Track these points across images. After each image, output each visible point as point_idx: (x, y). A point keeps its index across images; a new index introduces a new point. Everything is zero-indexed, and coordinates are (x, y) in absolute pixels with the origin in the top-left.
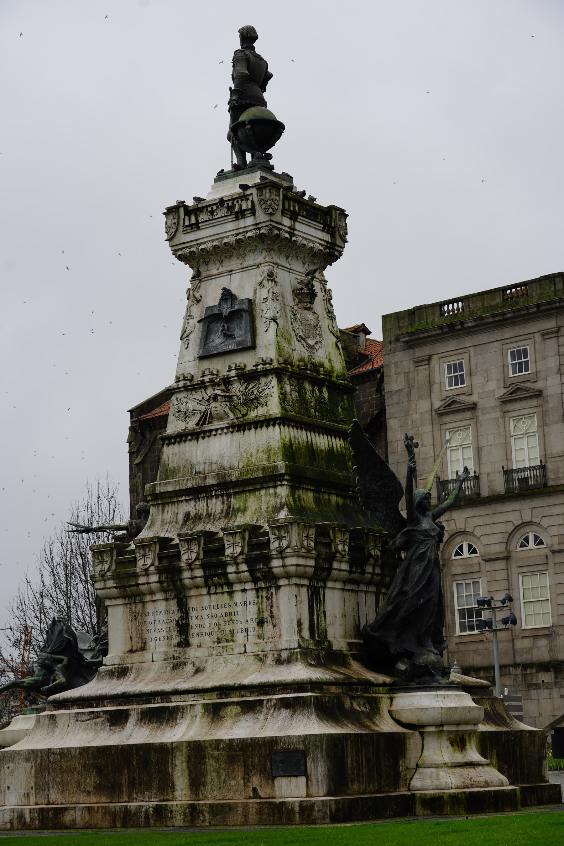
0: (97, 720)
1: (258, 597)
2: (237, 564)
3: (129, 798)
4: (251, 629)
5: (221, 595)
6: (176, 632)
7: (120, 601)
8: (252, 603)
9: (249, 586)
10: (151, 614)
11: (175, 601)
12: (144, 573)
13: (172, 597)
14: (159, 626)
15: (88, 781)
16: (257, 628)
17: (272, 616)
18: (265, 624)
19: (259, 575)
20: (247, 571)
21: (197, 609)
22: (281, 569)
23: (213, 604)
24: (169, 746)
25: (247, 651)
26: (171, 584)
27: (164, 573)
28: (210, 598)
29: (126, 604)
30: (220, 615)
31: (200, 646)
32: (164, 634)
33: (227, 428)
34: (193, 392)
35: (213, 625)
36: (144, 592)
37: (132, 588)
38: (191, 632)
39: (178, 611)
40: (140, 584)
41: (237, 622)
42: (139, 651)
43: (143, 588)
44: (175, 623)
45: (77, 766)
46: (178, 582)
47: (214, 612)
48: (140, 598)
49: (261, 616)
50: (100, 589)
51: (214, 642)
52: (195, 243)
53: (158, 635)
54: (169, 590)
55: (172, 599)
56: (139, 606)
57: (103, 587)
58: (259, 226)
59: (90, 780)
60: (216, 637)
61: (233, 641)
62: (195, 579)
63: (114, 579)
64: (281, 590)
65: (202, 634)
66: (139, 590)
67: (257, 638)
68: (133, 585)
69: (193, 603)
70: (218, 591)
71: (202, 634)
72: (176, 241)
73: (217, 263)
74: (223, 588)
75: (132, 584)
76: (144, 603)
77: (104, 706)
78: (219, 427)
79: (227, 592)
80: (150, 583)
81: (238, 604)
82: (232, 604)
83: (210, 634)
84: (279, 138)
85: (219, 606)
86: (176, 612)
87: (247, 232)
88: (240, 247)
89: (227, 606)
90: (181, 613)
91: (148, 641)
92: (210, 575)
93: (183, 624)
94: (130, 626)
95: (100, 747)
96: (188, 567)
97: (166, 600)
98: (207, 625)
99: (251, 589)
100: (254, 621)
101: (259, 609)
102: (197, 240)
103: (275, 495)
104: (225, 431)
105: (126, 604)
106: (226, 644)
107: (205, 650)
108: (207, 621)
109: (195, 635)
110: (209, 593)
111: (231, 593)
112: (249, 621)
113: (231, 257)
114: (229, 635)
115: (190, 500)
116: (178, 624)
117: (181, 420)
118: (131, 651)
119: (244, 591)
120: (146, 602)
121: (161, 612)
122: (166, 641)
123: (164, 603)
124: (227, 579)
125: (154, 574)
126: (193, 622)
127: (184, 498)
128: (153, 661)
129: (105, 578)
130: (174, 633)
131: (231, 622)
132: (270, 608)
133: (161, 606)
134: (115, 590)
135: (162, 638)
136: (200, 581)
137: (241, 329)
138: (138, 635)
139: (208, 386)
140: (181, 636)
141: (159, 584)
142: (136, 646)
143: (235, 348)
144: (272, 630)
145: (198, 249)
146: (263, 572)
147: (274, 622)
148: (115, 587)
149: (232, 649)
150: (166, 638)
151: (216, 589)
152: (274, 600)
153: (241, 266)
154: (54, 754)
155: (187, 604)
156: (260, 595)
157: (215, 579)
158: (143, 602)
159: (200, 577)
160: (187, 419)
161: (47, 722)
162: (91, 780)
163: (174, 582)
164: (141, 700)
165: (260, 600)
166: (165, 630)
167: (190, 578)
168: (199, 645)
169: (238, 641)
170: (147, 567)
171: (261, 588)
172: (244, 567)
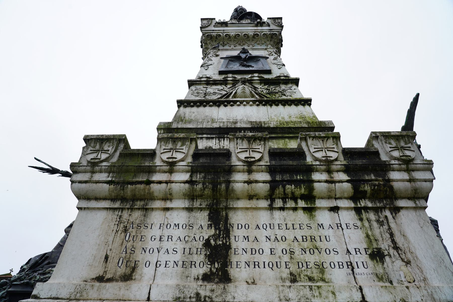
1: (361, 220)
2: (329, 172)
4: (360, 264)
5: (291, 212)
6: (202, 256)
8: (351, 226)
11: (205, 214)
12: (167, 168)
13: (204, 206)
14: (168, 245)
16: (370, 263)
17: (396, 248)
18: (387, 258)
19: (367, 188)
20: (348, 181)
21: (247, 227)
22: (407, 184)
23: (276, 223)
26: (210, 186)
27: (200, 172)
28: (272, 214)
29: (114, 209)
30: (292, 238)
31: (253, 283)
32: (178, 257)
33: (254, 102)
36: (156, 194)
37: (138, 186)
38: (234, 259)
39: (210, 226)
40: (153, 182)
41: (328, 251)
42: (117, 281)
44: (201, 243)
46: (223, 186)
47: (280, 233)
48: (142, 203)
49: (375, 246)
51: (283, 280)
53: (163, 258)
54: (201, 196)
56: (137, 215)
60: (287, 271)
61: (323, 280)
62: (254, 185)
63: (109, 173)
65: (256, 265)
66: (149, 190)
67: (376, 279)
68: (141, 183)
70: (288, 205)
71: (256, 265)
74: (296, 203)
75: (140, 179)
76: (146, 210)
79: (304, 209)
82: (314, 226)
83: (276, 265)
85: (290, 225)
86: (205, 228)
89: (305, 226)
90: (216, 229)
91: (141, 265)
92: (283, 181)
93: (216, 246)
94: (111, 239)
96: (246, 168)
97: (190, 210)
99: (348, 209)
100: (363, 252)
101: (368, 236)
104: (251, 103)
105: (114, 209)
106: (310, 284)
107: (270, 289)
108: (266, 246)
109: (243, 264)
110: (271, 208)
111: (310, 211)
112: (353, 252)
114: (315, 271)
115: (212, 138)
116: (207, 244)
118: (100, 279)
119: (335, 209)
120: (153, 209)
121: (177, 226)
122: (179, 269)
124: (311, 189)
125: (183, 171)
127: (205, 136)
129: (97, 168)
130: (199, 258)
131: (316, 251)
132: (388, 236)
134: (106, 186)
135: (171, 264)
136: (263, 188)
138: (124, 255)
140: (212, 263)
141: (187, 185)
142: (113, 271)
144: (404, 268)
146: (375, 185)
147: (403, 257)
148: (109, 182)
149: (333, 293)
150: (180, 263)
151: (285, 202)
152: (393, 225)
155: (227, 218)
157: (290, 188)
158: (147, 209)
159: (264, 182)
163: (215, 185)
165: (366, 224)
166: (180, 251)
167: (245, 182)
168: (250, 281)
169: (334, 280)
171: (366, 209)
172: (343, 176)
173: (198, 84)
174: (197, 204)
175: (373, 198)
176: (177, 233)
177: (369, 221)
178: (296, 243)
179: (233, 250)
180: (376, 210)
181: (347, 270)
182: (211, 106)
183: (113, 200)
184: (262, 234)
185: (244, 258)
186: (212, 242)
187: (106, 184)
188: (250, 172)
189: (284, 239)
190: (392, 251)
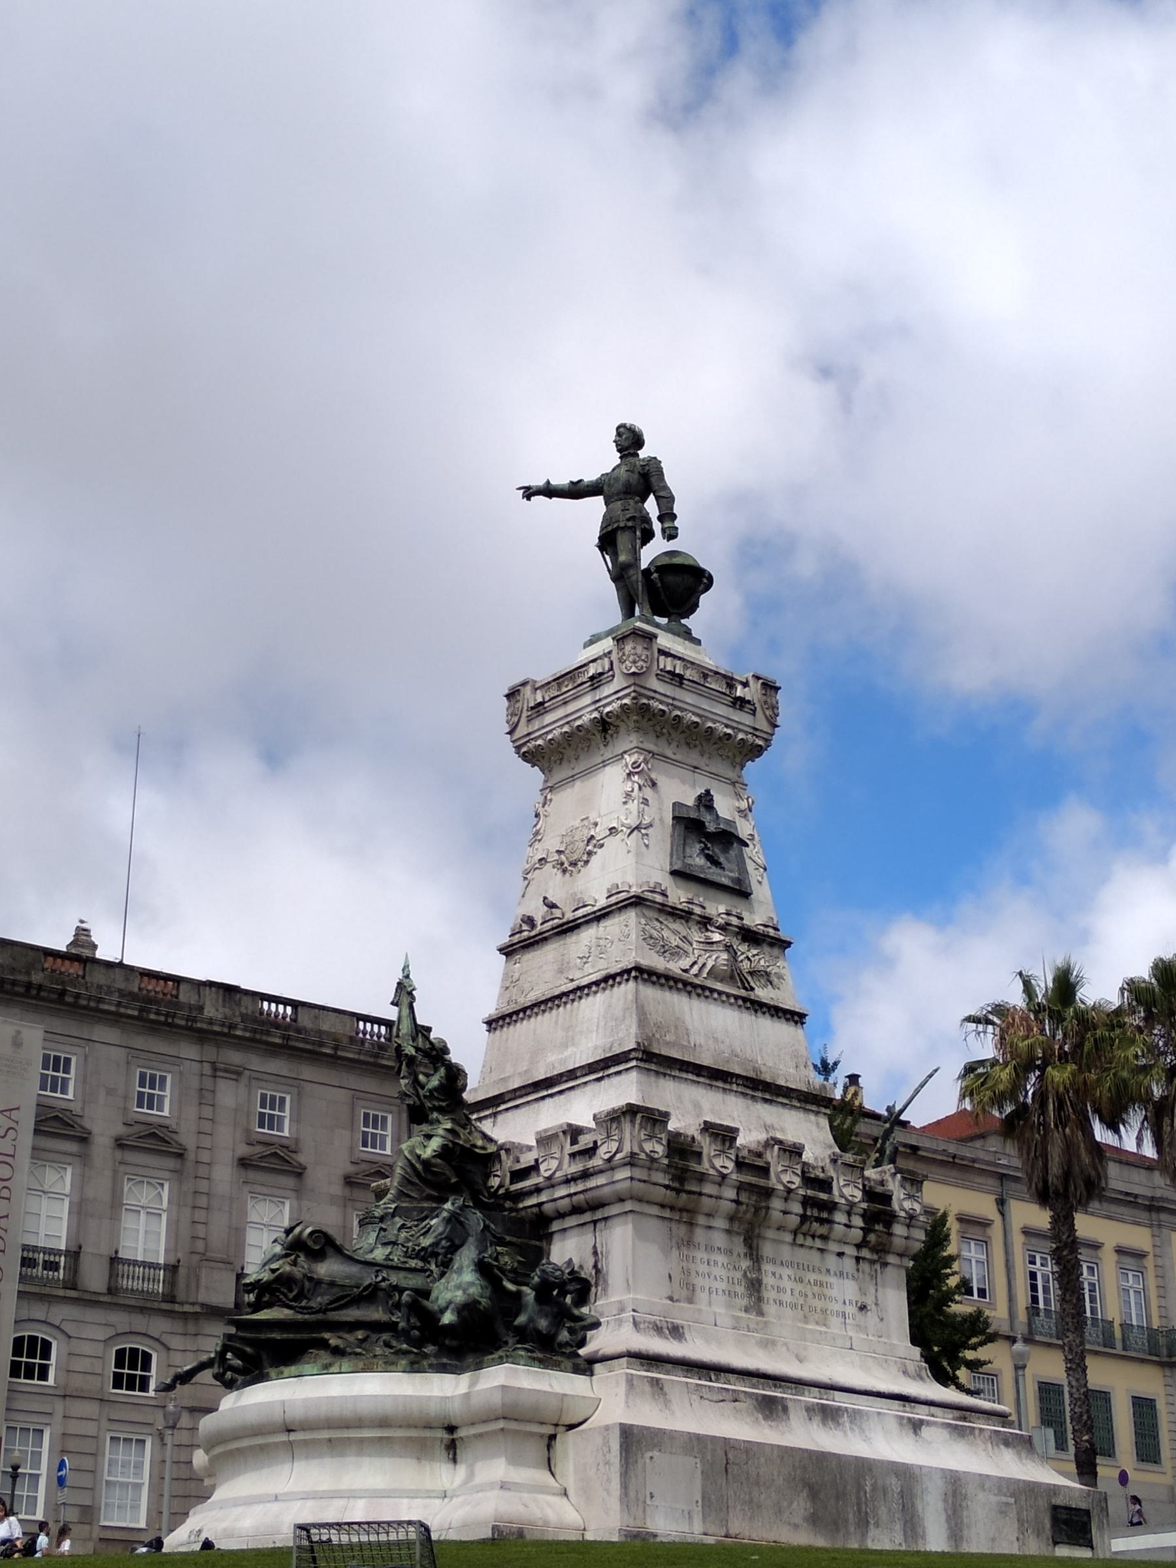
6: (743, 1288)
9: (851, 1251)
35: (796, 1293)
38: (765, 1294)
41: (831, 1299)
50: (640, 1180)
55: (738, 1233)
85: (806, 1266)
86: (742, 1256)
99: (851, 1256)
119: (840, 1254)
121: (719, 1249)
126: (768, 1280)
130: (740, 1289)
133: (719, 1239)
135: (720, 1292)
166: (726, 1280)
171: (864, 1259)
175: (873, 1250)
178: (809, 1286)
179: (763, 1286)
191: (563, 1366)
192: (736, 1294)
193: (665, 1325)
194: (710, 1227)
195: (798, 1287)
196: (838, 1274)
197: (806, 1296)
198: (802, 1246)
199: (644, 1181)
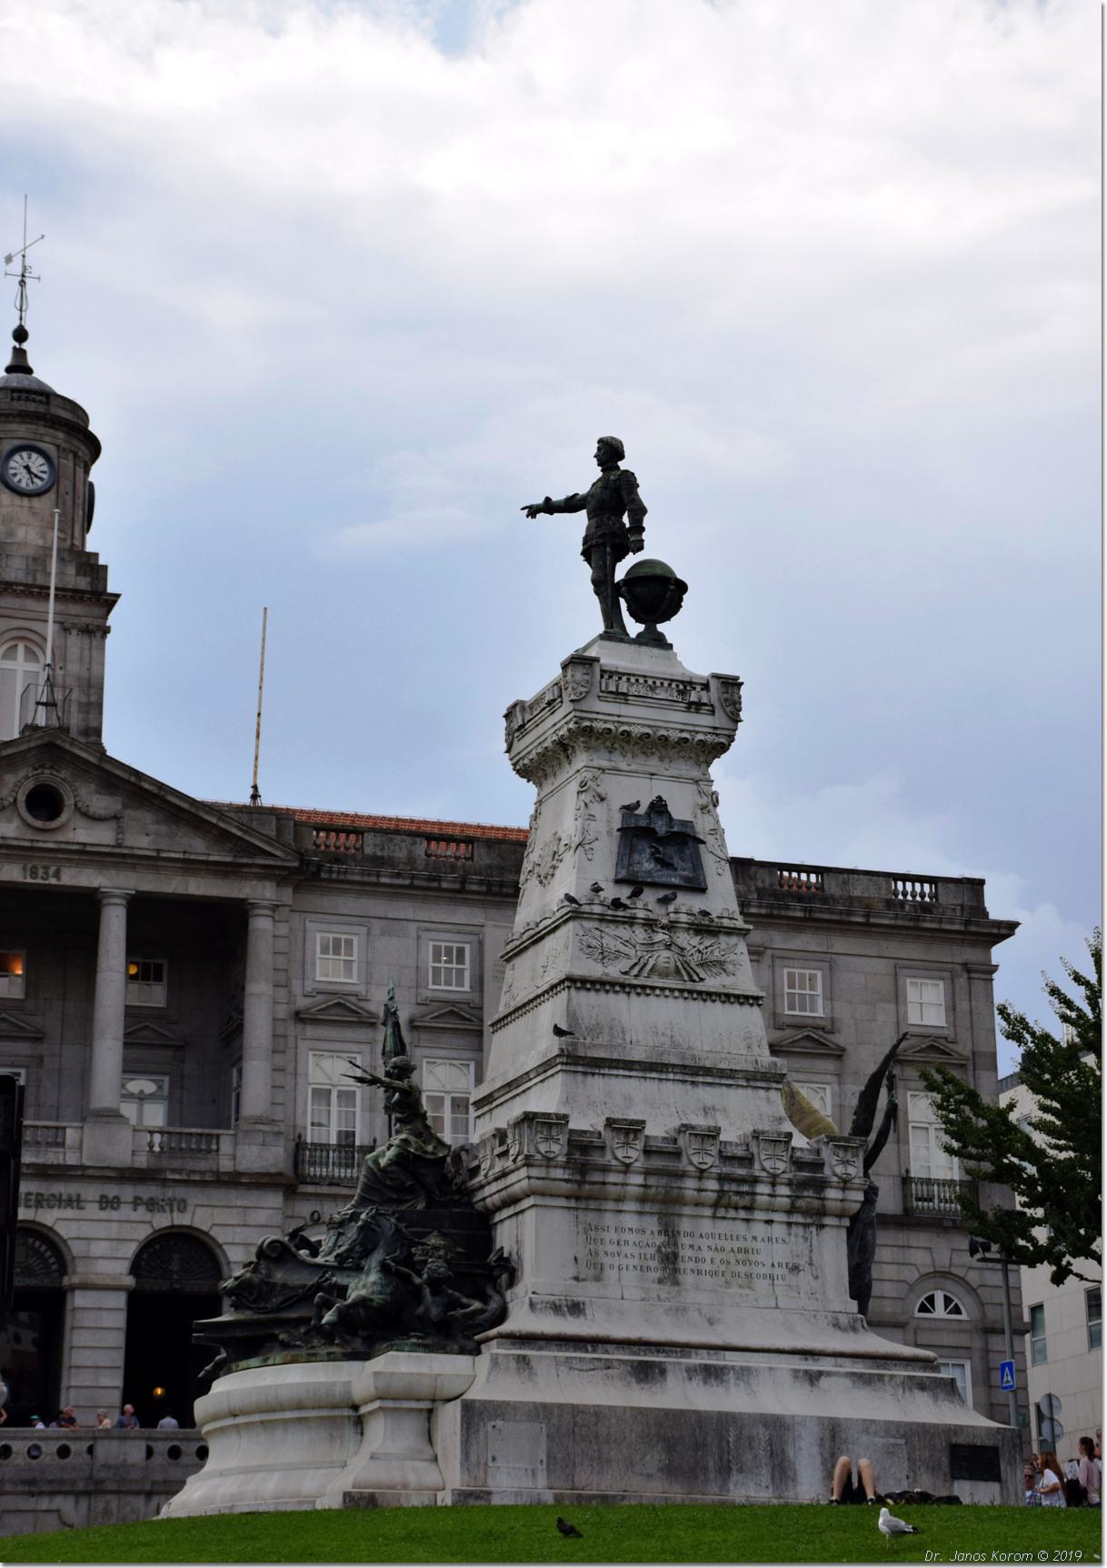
0: (609, 1371)
1: (790, 1234)
2: (773, 1185)
3: (721, 1490)
7: (562, 1202)
10: (612, 1230)
14: (627, 1250)
15: (648, 1458)
17: (811, 1264)
20: (788, 1196)
21: (692, 1235)
22: (839, 1203)
24: (788, 1422)
25: (780, 1306)
29: (569, 1208)
33: (681, 991)
34: (612, 926)
38: (681, 1266)
41: (757, 1263)
43: (611, 1188)
45: (627, 1434)
47: (720, 1243)
52: (616, 719)
53: (624, 1262)
57: (543, 1176)
58: (718, 732)
59: (652, 1457)
64: (824, 1231)
65: (699, 1272)
69: (685, 1225)
71: (699, 1272)
72: (584, 705)
73: (629, 755)
77: (607, 1352)
78: (660, 985)
80: (627, 1185)
81: (759, 1239)
82: (749, 1238)
84: (676, 613)
85: (728, 1236)
86: (656, 1234)
87: (697, 732)
88: (674, 747)
91: (606, 1268)
95: (671, 1410)
97: (640, 1213)
98: (709, 1261)
102: (619, 716)
103: (768, 1100)
105: (569, 1208)
110: (714, 1217)
113: (652, 754)
116: (659, 1250)
117: (595, 960)
119: (769, 1222)
120: (606, 1210)
121: (631, 1229)
123: (635, 1217)
124: (753, 1201)
126: (685, 1252)
128: (622, 1298)
129: (553, 1163)
130: (653, 1264)
133: (630, 1221)
135: (631, 1268)
136: (711, 1196)
137: (683, 860)
139: (637, 923)
141: (642, 1189)
143: (682, 883)
145: (617, 729)
148: (567, 1181)
149: (756, 1300)
152: (814, 1242)
153: (667, 773)
154: (582, 1412)
156: (793, 1232)
159: (712, 1191)
160: (605, 961)
161: (513, 1365)
162: (655, 1458)
164: (672, 1352)
170: (631, 1161)
173: (586, 918)
174: (647, 1208)
176: (632, 1238)
177: (796, 1236)
178: (732, 1254)
180: (805, 1226)
181: (768, 1281)
182: (616, 992)
183: (567, 1197)
184: (705, 1243)
185: (690, 1265)
186: (663, 1249)
187: (563, 1184)
188: (700, 1178)
189: (723, 1250)
190: (807, 1267)
191: (448, 1349)
192: (648, 1268)
193: (564, 1303)
194: (621, 1211)
195: (719, 1256)
196: (766, 1239)
197: (729, 1263)
198: (724, 1218)
199: (543, 1179)
